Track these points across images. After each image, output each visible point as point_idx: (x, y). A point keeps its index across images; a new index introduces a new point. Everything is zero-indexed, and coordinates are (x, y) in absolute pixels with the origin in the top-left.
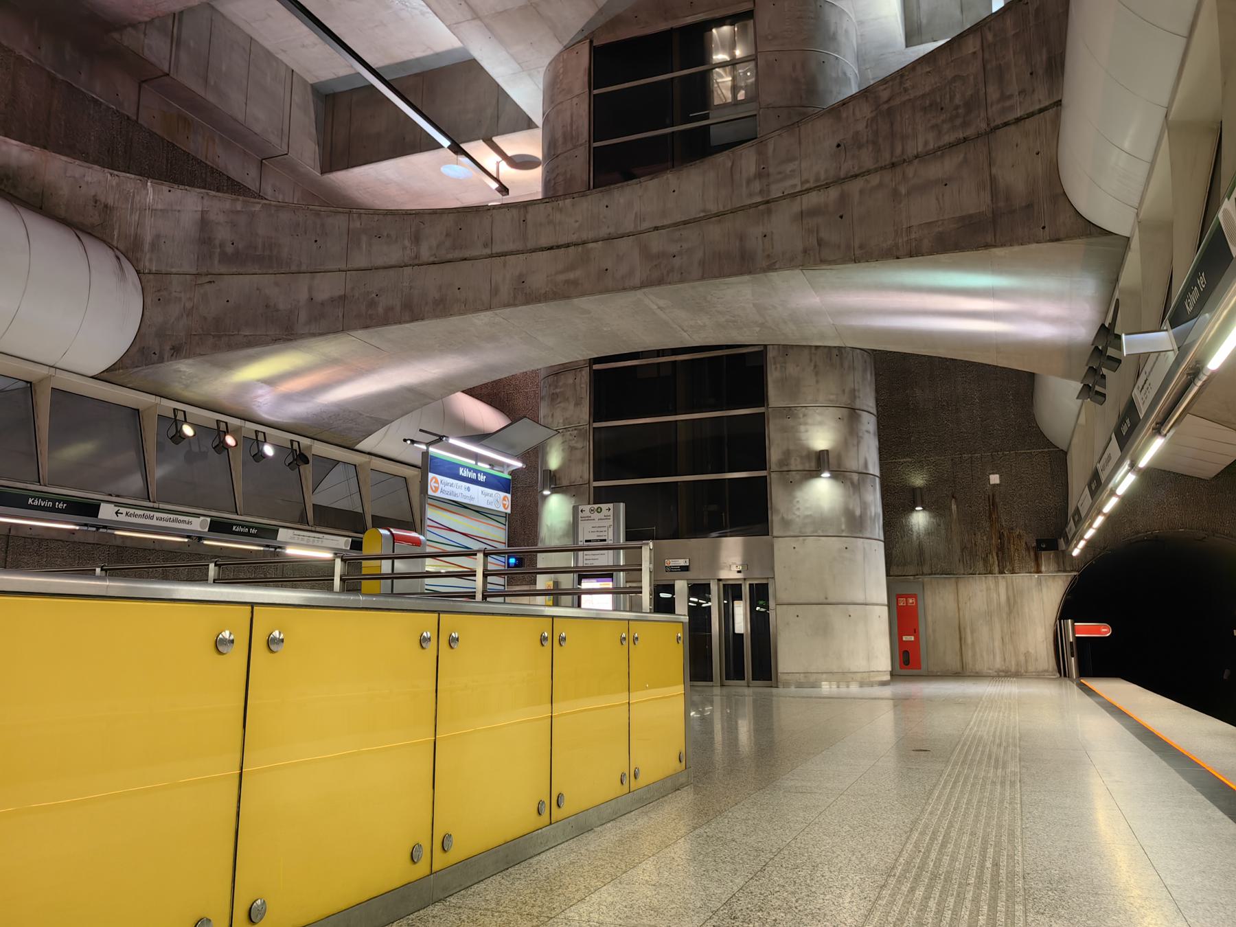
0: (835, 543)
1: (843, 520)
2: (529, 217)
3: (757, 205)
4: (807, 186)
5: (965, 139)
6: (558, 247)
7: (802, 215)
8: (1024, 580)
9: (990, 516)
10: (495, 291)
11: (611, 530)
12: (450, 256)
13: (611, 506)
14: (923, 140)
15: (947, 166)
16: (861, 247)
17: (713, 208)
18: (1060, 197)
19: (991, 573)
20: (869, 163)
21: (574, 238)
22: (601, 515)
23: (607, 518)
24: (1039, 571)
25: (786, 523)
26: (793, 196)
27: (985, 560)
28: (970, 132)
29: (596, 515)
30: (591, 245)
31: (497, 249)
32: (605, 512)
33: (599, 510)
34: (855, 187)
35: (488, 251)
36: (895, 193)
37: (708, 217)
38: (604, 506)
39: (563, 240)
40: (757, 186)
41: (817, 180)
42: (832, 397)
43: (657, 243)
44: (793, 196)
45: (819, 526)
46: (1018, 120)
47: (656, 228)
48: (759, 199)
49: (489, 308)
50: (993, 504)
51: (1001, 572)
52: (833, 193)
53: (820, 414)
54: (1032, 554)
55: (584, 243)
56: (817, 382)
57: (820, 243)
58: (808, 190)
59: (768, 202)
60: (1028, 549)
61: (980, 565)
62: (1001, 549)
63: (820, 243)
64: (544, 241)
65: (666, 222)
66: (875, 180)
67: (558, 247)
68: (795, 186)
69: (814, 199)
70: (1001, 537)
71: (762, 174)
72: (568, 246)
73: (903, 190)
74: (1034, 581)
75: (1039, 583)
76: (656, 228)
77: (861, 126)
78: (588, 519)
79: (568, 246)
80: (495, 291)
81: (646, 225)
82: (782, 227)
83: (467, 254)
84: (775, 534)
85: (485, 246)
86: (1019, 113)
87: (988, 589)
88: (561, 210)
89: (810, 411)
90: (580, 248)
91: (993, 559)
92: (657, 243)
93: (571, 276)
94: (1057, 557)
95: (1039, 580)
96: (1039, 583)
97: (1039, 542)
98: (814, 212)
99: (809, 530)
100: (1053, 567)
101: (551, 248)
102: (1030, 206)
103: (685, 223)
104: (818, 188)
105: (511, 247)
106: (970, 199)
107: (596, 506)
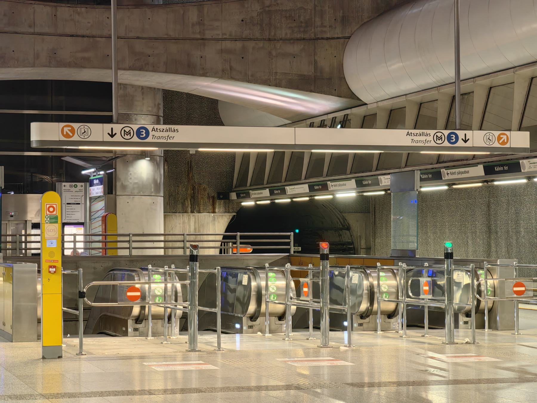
0: (148, 200)
1: (153, 185)
2: (58, 13)
3: (197, 39)
4: (225, 37)
5: (304, 39)
6: (77, 36)
7: (222, 51)
8: (205, 217)
9: (188, 175)
10: (37, 56)
11: (83, 198)
12: (7, 29)
13: (83, 184)
14: (283, 32)
15: (295, 48)
16: (252, 76)
17: (172, 34)
18: (342, 79)
19: (186, 212)
20: (258, 35)
21: (87, 32)
22: (77, 189)
23: (80, 191)
24: (214, 212)
25: (124, 187)
26: (218, 40)
27: (183, 204)
28: (307, 36)
29: (73, 189)
30: (98, 39)
31: (37, 30)
32: (79, 187)
33: (76, 186)
34: (250, 45)
35: (31, 30)
36: (270, 53)
37: (170, 39)
38: (79, 184)
39: (80, 32)
40: (197, 29)
41: (230, 35)
42: (150, 109)
43: (139, 46)
44: (218, 40)
45: (141, 190)
46: (328, 39)
47: (138, 38)
48: (199, 37)
49: (33, 66)
50: (190, 168)
51: (192, 212)
52: (239, 44)
53: (144, 119)
54: (211, 201)
55: (93, 37)
56: (143, 99)
57: (231, 68)
58: (225, 39)
59: (203, 39)
60: (209, 197)
61: (180, 206)
62: (193, 197)
63: (231, 68)
64: (68, 31)
65: (145, 35)
66: (261, 44)
67: (77, 36)
68: (219, 35)
69: (228, 45)
70: (194, 189)
71: (201, 23)
72: (83, 36)
73: (274, 53)
74: (211, 219)
75: (214, 219)
76: (138, 38)
77: (255, 14)
78: (69, 191)
79: (83, 36)
80: (37, 56)
81: (132, 35)
82: (211, 53)
83: (18, 30)
84: (118, 193)
85: (30, 26)
86: (328, 35)
87: (184, 223)
88: (79, 14)
89: (139, 117)
90: (91, 39)
91: (188, 203)
92: (139, 46)
93: (86, 55)
94: (225, 203)
95: (214, 217)
96: (214, 219)
97: (219, 194)
98: (229, 51)
99: (136, 192)
100: (222, 209)
101: (72, 36)
102: (330, 79)
103: (156, 39)
104: (231, 40)
105: (46, 30)
106: (307, 69)
107: (74, 184)
